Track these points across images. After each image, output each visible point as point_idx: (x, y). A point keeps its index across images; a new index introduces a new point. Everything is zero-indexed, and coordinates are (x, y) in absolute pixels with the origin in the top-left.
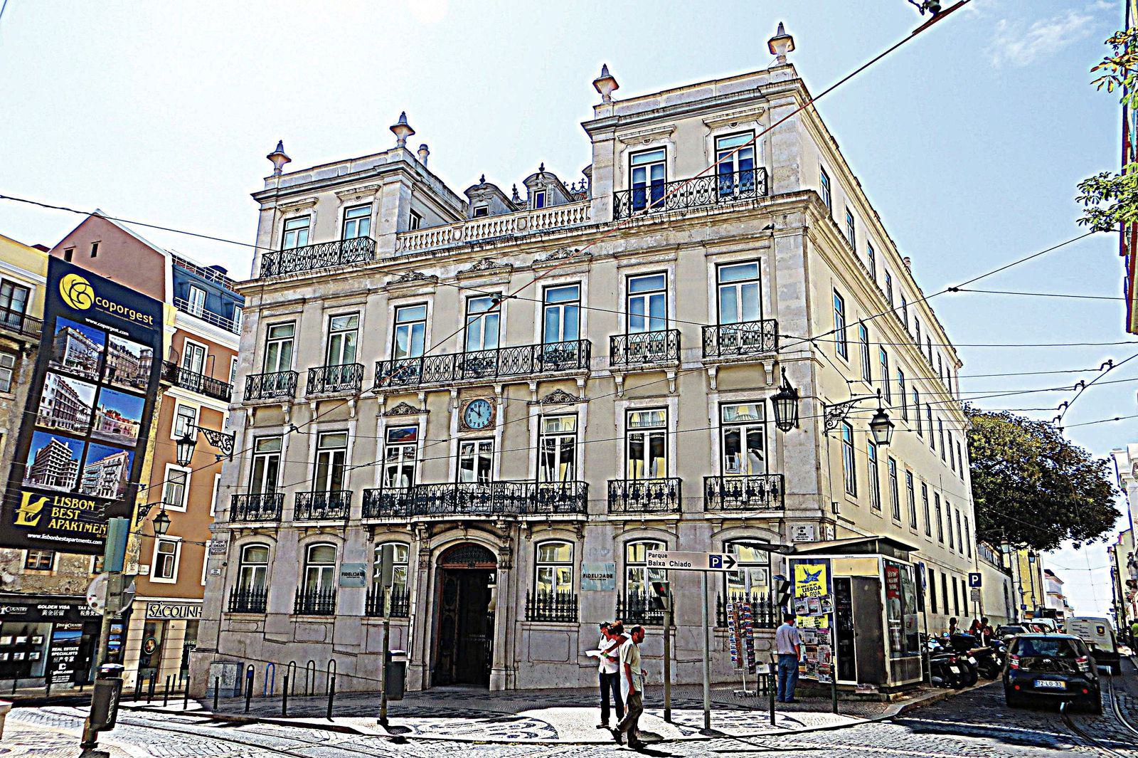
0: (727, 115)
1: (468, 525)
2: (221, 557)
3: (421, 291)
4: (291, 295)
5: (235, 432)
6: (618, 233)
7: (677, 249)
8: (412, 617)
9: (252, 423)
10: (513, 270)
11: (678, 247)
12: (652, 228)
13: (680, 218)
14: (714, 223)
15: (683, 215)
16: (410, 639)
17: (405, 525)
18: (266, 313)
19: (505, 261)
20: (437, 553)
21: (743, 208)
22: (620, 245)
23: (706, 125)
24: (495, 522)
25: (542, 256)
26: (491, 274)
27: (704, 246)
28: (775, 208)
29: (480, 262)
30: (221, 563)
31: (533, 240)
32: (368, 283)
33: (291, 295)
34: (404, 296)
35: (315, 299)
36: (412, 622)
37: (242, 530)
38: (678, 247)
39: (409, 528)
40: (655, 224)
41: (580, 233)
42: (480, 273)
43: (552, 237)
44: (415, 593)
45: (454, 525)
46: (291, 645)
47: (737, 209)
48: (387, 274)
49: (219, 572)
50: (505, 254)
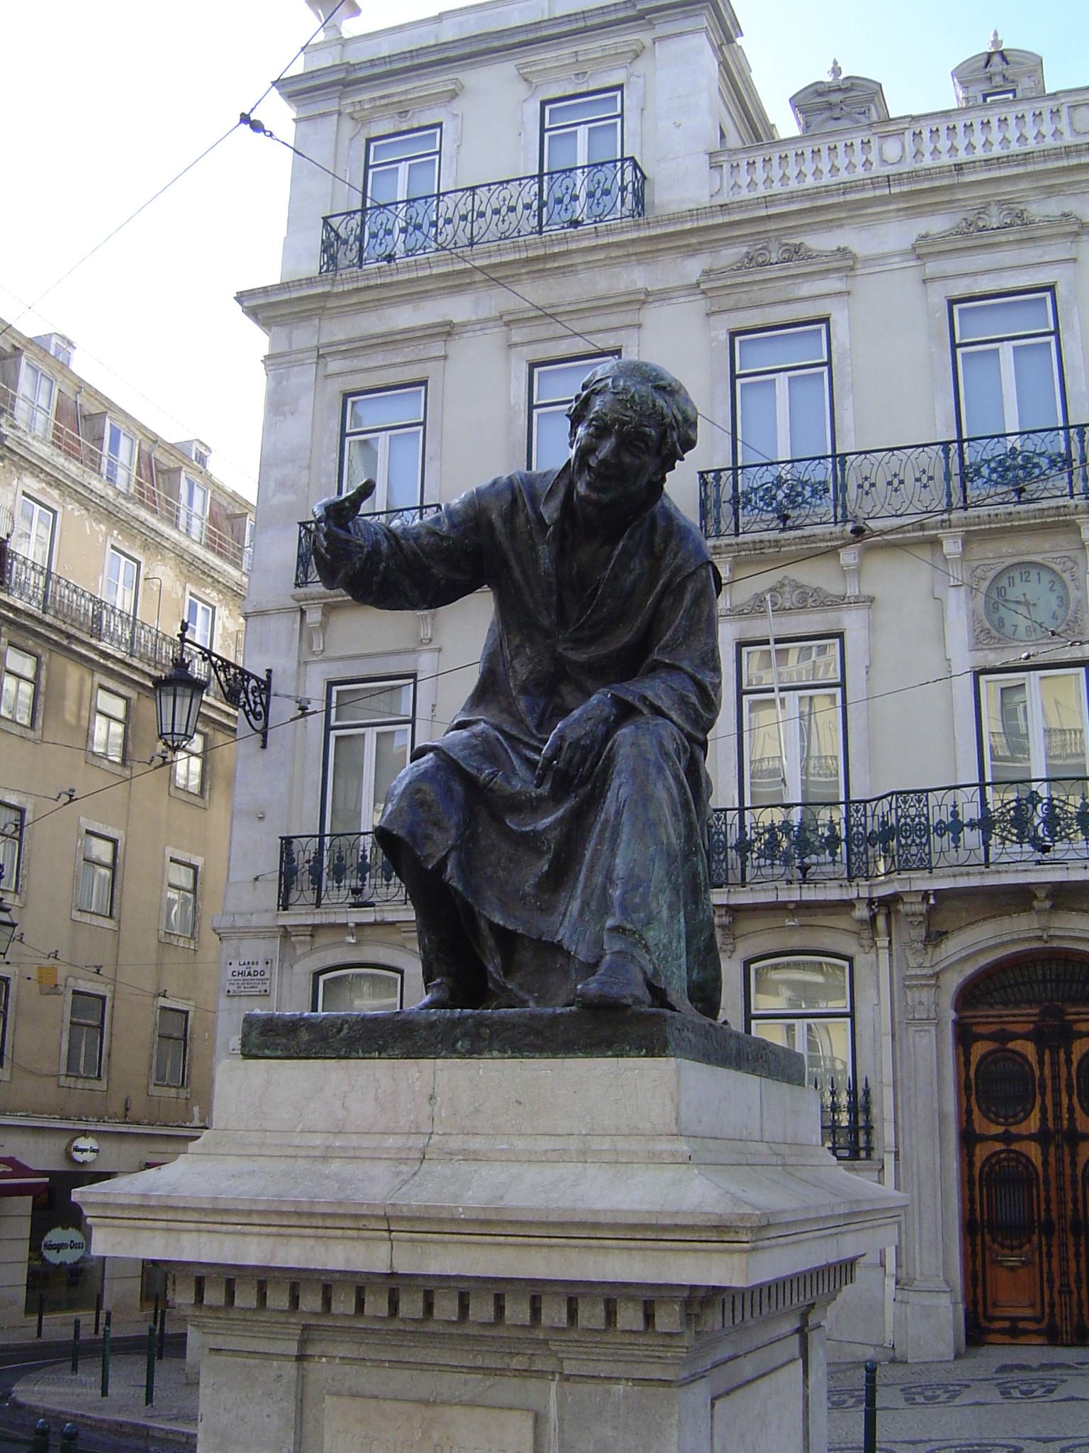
3: (806, 289)
4: (405, 317)
5: (269, 671)
8: (889, 1160)
17: (848, 905)
18: (335, 365)
19: (1053, 207)
20: (953, 981)
32: (638, 278)
33: (405, 317)
35: (484, 323)
37: (316, 928)
39: (862, 912)
44: (888, 1093)
45: (1019, 898)
48: (693, 251)
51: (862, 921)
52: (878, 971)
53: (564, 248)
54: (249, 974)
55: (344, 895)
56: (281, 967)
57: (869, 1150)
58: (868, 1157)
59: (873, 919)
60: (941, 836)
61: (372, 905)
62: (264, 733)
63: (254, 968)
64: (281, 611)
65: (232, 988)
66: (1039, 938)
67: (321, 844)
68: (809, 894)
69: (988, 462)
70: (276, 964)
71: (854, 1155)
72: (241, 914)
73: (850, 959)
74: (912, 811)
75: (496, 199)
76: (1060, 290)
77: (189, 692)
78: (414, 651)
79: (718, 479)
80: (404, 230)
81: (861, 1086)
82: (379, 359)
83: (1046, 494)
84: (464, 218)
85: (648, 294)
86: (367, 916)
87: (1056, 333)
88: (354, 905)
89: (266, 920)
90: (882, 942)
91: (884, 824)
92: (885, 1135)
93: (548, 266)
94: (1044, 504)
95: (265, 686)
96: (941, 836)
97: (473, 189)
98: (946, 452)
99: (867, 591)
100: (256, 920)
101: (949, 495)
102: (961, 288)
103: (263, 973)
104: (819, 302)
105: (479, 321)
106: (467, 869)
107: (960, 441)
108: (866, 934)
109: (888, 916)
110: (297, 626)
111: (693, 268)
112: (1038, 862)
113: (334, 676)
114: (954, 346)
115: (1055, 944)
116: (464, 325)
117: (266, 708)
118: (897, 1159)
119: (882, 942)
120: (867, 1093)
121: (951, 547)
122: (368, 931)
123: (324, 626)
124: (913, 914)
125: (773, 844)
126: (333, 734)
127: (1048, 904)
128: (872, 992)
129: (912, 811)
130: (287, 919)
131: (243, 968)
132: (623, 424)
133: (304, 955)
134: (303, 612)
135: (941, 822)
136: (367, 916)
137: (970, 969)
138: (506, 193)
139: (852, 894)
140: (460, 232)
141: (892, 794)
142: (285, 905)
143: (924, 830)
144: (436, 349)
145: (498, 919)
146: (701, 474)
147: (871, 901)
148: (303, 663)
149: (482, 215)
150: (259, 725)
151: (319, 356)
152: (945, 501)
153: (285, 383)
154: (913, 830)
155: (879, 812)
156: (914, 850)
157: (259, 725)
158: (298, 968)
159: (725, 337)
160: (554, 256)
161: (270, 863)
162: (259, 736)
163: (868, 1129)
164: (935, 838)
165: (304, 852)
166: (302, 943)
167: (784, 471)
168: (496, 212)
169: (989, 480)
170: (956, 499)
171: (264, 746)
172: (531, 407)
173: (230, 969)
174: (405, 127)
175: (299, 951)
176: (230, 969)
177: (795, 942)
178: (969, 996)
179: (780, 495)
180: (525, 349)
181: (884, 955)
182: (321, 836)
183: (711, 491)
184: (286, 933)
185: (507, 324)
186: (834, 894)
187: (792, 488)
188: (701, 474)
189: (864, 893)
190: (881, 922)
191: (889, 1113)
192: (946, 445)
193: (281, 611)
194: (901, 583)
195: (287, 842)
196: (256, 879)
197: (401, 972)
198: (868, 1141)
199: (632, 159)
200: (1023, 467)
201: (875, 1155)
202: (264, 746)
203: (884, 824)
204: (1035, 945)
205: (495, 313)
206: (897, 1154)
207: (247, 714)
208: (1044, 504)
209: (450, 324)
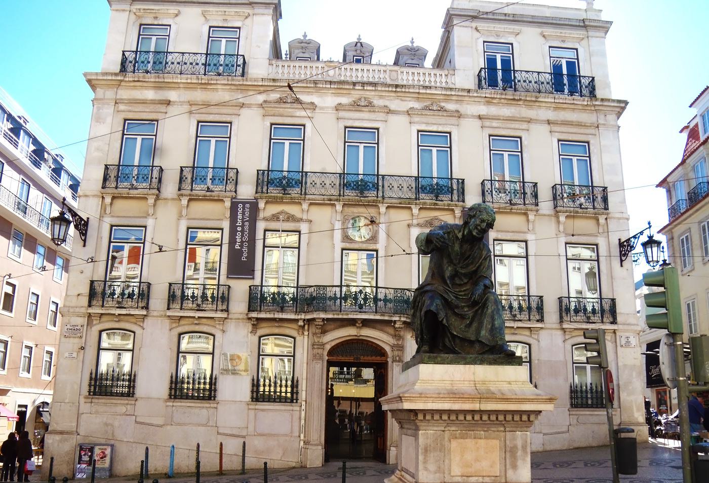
0: (561, 33)
1: (366, 323)
2: (77, 340)
5: (88, 218)
6: (483, 100)
7: (529, 122)
8: (304, 403)
9: (108, 211)
10: (390, 112)
11: (530, 121)
12: (509, 102)
13: (534, 99)
14: (556, 109)
15: (536, 97)
16: (303, 422)
17: (297, 321)
20: (328, 347)
21: (580, 103)
22: (483, 110)
23: (544, 36)
24: (395, 322)
25: (417, 105)
26: (370, 111)
27: (549, 124)
28: (600, 108)
29: (360, 99)
30: (77, 347)
31: (411, 90)
34: (282, 116)
36: (303, 407)
38: (530, 121)
40: (514, 99)
41: (453, 93)
42: (360, 108)
43: (428, 91)
44: (304, 382)
45: (352, 322)
46: (169, 427)
47: (576, 102)
49: (75, 355)
50: (381, 97)
51: (300, 326)
52: (304, 342)
53: (215, 82)
55: (115, 304)
56: (87, 328)
57: (297, 400)
58: (297, 402)
59: (304, 325)
60: (330, 301)
61: (125, 308)
62: (85, 241)
63: (76, 327)
64: (94, 196)
65: (66, 334)
66: (356, 336)
67: (105, 285)
68: (284, 316)
69: (353, 182)
70: (85, 327)
71: (292, 401)
72: (72, 307)
73: (294, 338)
74: (321, 292)
75: (192, 59)
76: (381, 130)
77: (59, 222)
78: (146, 217)
79: (263, 174)
80: (149, 62)
81: (295, 379)
82: (140, 108)
83: (370, 195)
84: (178, 63)
85: (243, 104)
86: (123, 312)
87: (378, 144)
88: (118, 308)
89: (83, 310)
90: (306, 333)
91: (311, 295)
92: (303, 395)
93: (208, 87)
94: (370, 198)
95: (86, 224)
96: (330, 301)
97: (183, 53)
98: (340, 177)
99: (310, 218)
100: (77, 310)
101: (340, 191)
102: (349, 123)
104: (302, 119)
105: (180, 102)
106: (447, 321)
107: (344, 174)
108: (301, 331)
109: (309, 325)
110: (100, 203)
111: (261, 98)
112: (360, 312)
113: (113, 223)
114: (345, 142)
115: (360, 338)
116: (174, 102)
117: (86, 231)
118: (306, 403)
119: (306, 333)
120: (297, 381)
121: (339, 207)
122: (122, 317)
123: (111, 204)
124: (319, 325)
125: (274, 299)
126: (112, 244)
127: (361, 325)
128: (301, 349)
129: (321, 292)
130: (91, 311)
131: (71, 328)
132: (488, 220)
133: (95, 324)
134: (103, 198)
135: (330, 296)
136: (123, 312)
137: (333, 344)
138: (195, 58)
139: (299, 317)
140: (177, 68)
141: (315, 286)
142: (90, 306)
143: (324, 298)
144: (163, 108)
145: (455, 333)
146: (258, 170)
147: (304, 320)
148: (101, 216)
149: (185, 64)
150: (83, 238)
151: (116, 103)
152: (338, 192)
153: (101, 111)
154: (321, 298)
155: (310, 291)
156: (321, 305)
157: (83, 238)
159: (269, 125)
160: (211, 84)
161: (86, 290)
162: (82, 243)
163: (297, 393)
164: (328, 302)
165: (99, 288)
166: (96, 320)
167: (285, 174)
168: (191, 64)
169: (353, 188)
170: (342, 193)
171: (84, 246)
172: (197, 137)
173: (66, 327)
174: (156, 23)
175: (95, 322)
176: (67, 327)
177: (276, 331)
178: (331, 352)
179: (284, 182)
180: (197, 115)
181: (306, 337)
182: (105, 281)
183: (260, 177)
184: (90, 315)
185: (191, 105)
186: (292, 316)
187: (288, 180)
188: (258, 170)
189: (303, 317)
190: (306, 327)
191: (304, 388)
192: (340, 174)
193: (94, 196)
194: (322, 216)
195: (92, 282)
197: (134, 332)
198: (297, 397)
199: (243, 56)
200: (364, 186)
201: (298, 401)
202: (84, 246)
203: (311, 295)
204: (356, 338)
205: (186, 100)
206: (306, 401)
207: (80, 233)
208: (370, 198)
209: (170, 101)
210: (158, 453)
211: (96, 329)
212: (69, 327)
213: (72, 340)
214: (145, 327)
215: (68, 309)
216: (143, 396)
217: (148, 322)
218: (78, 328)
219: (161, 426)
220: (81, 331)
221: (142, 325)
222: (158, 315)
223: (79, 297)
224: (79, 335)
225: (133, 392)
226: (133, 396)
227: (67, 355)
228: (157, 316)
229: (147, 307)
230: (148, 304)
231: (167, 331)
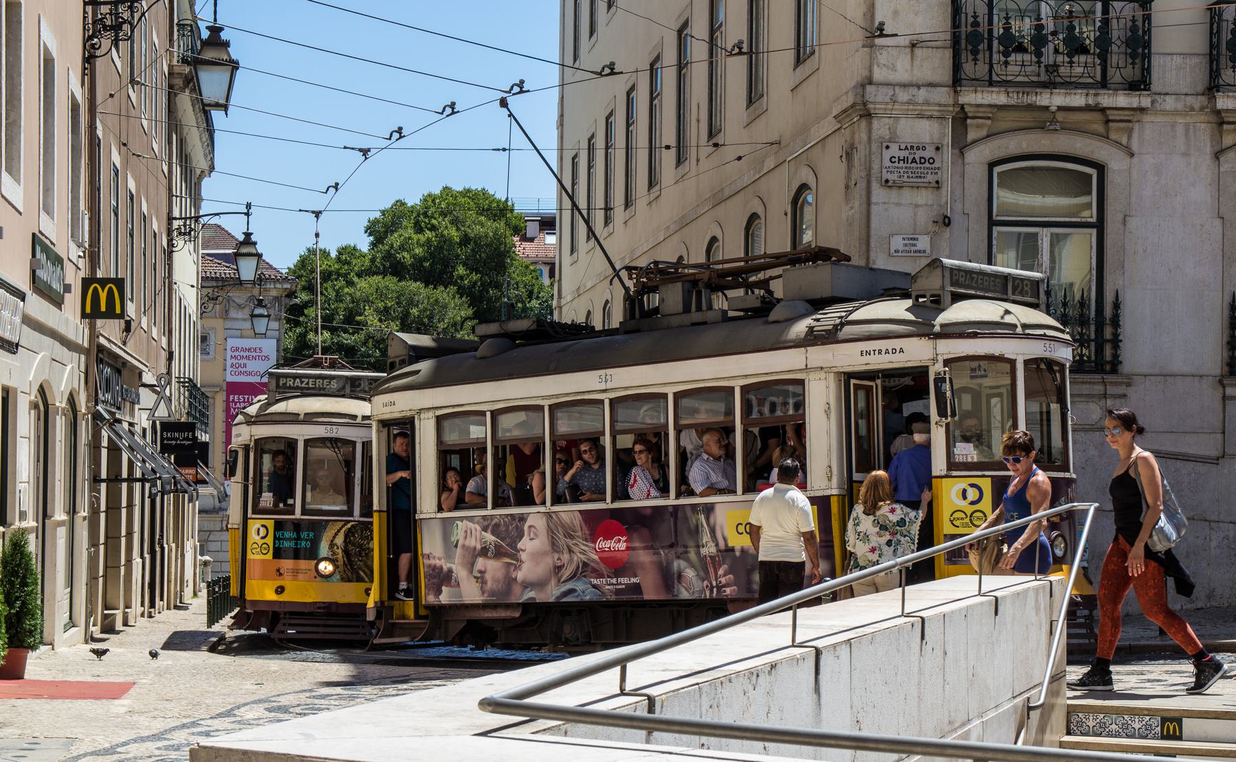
2: (924, 197)
30: (924, 218)
54: (914, 161)
103: (932, 161)
131: (903, 154)
158: (972, 156)
173: (887, 155)
176: (887, 155)
196: (913, 46)
210: (1214, 544)
211: (978, 156)
212: (894, 151)
213: (907, 196)
214: (1135, 146)
215: (891, 92)
216: (1145, 370)
217: (1146, 134)
218: (927, 154)
219: (1215, 461)
220: (936, 165)
221: (1124, 141)
222: (1180, 106)
223: (918, 52)
224: (930, 178)
225: (1116, 356)
226: (1114, 371)
227: (897, 243)
228: (1175, 113)
229: (1140, 84)
230: (1146, 71)
231: (1206, 160)
